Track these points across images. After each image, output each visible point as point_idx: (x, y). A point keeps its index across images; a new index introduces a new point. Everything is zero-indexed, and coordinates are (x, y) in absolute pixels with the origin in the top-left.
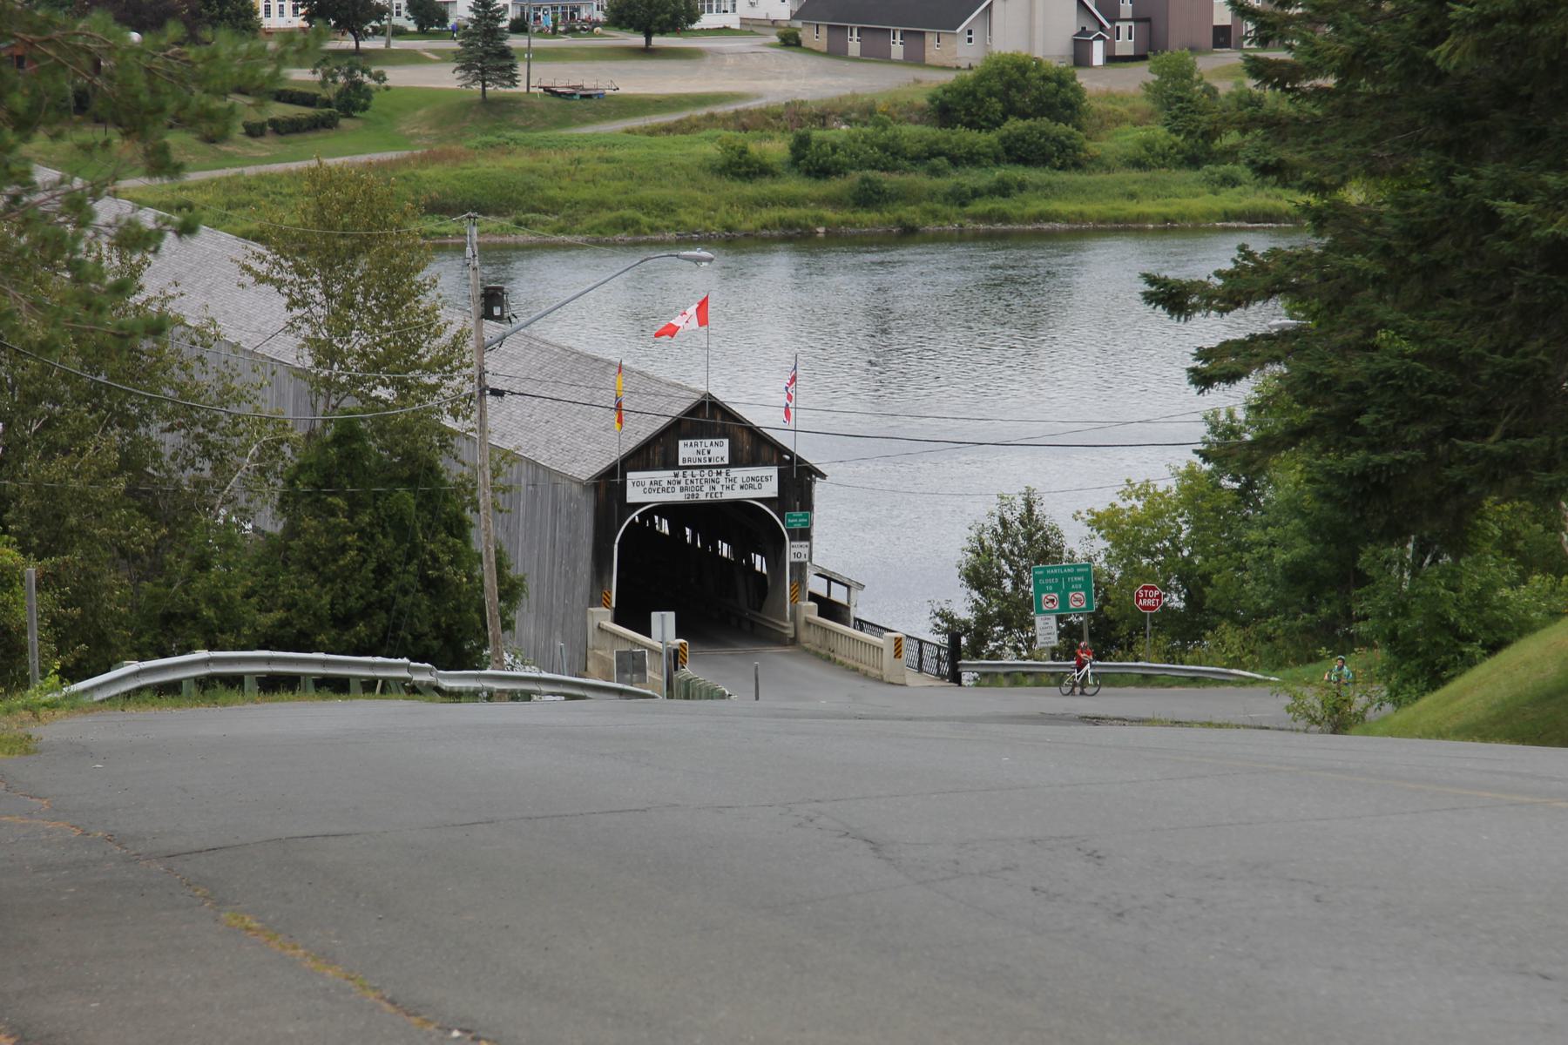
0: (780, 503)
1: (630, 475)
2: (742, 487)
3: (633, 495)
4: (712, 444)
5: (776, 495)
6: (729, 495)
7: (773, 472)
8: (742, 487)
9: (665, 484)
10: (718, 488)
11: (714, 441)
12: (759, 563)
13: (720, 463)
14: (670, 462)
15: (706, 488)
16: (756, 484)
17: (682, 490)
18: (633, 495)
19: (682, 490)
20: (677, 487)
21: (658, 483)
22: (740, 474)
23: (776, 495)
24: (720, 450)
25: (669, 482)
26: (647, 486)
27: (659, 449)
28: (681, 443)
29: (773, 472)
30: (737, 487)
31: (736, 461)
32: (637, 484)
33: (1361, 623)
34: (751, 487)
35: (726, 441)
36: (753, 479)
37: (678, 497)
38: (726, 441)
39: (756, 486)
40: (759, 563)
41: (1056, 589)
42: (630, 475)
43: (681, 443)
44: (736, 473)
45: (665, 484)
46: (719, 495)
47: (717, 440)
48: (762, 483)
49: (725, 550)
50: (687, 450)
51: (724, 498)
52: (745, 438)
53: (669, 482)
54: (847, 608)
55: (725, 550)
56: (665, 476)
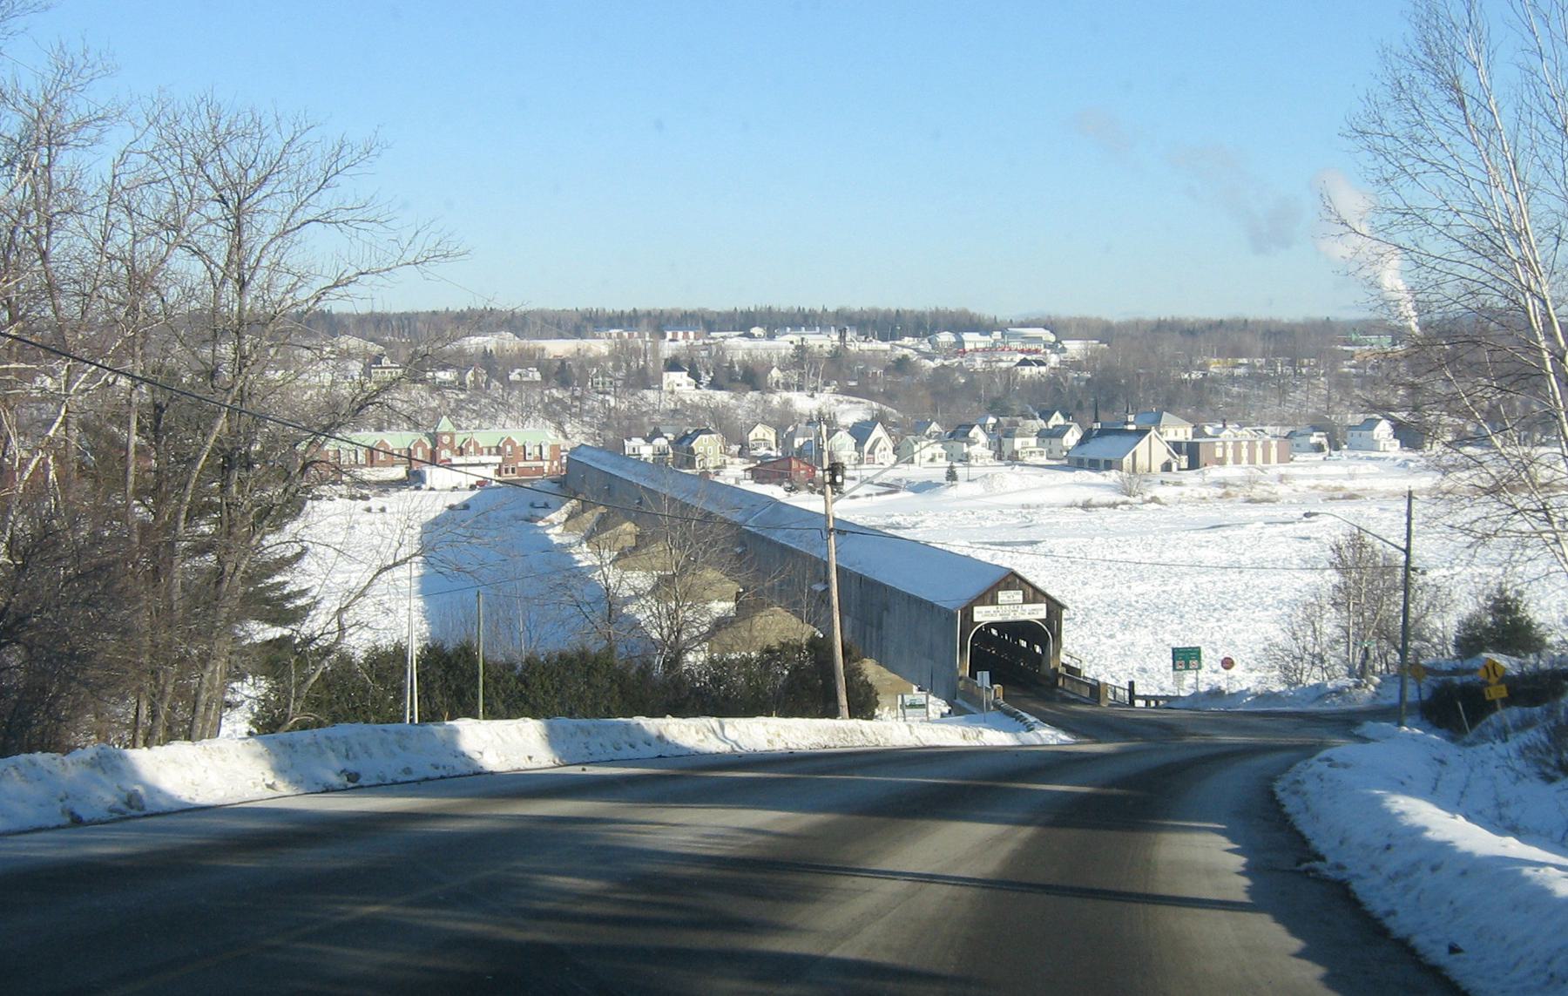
0: (1046, 621)
1: (976, 609)
7: (1044, 606)
12: (1038, 649)
14: (994, 602)
15: (1012, 614)
24: (1018, 596)
27: (990, 595)
28: (1000, 593)
31: (1026, 601)
33: (1415, 687)
35: (1021, 592)
37: (998, 618)
38: (1021, 592)
40: (1038, 649)
41: (1183, 659)
42: (976, 609)
43: (1000, 593)
44: (1025, 606)
48: (1037, 612)
49: (1024, 644)
50: (1003, 596)
52: (1030, 591)
54: (1080, 671)
55: (1024, 644)
56: (993, 608)
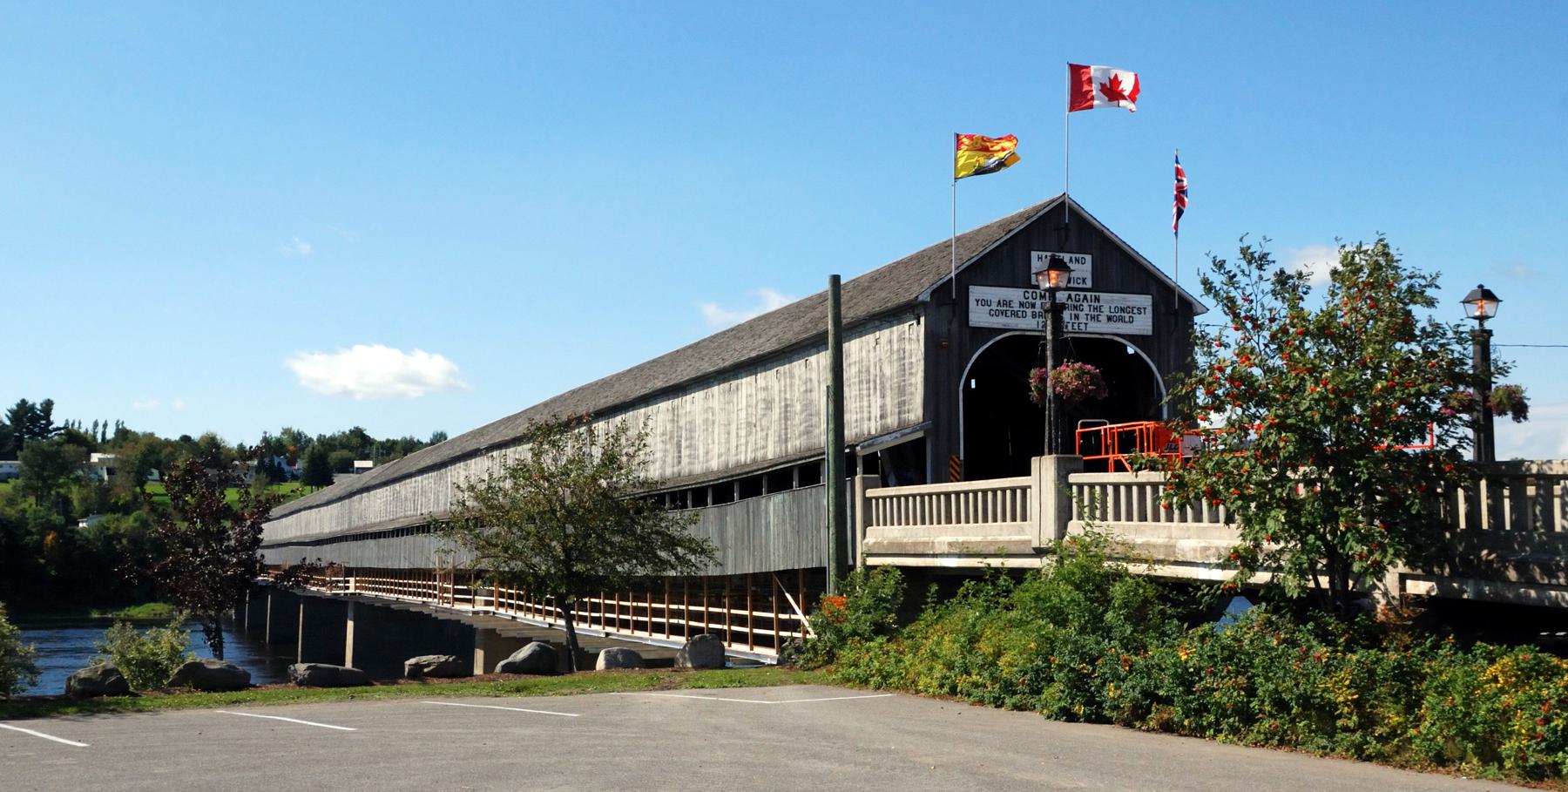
1: (976, 292)
2: (1109, 319)
3: (979, 317)
4: (1071, 260)
5: (1150, 333)
6: (1093, 327)
7: (1145, 301)
8: (1109, 319)
9: (1016, 307)
10: (1082, 319)
11: (1074, 256)
13: (1081, 286)
16: (1127, 315)
17: (1034, 316)
18: (979, 317)
19: (1034, 316)
20: (1029, 311)
21: (1008, 303)
22: (1109, 300)
23: (1150, 333)
25: (1021, 305)
26: (994, 307)
29: (1145, 301)
30: (1103, 318)
31: (1102, 282)
32: (985, 303)
34: (1121, 319)
35: (1088, 258)
36: (1122, 310)
38: (1088, 258)
39: (1127, 319)
42: (976, 292)
45: (1016, 307)
46: (1082, 327)
47: (1078, 256)
51: (1089, 330)
53: (1021, 305)
56: (1015, 295)
